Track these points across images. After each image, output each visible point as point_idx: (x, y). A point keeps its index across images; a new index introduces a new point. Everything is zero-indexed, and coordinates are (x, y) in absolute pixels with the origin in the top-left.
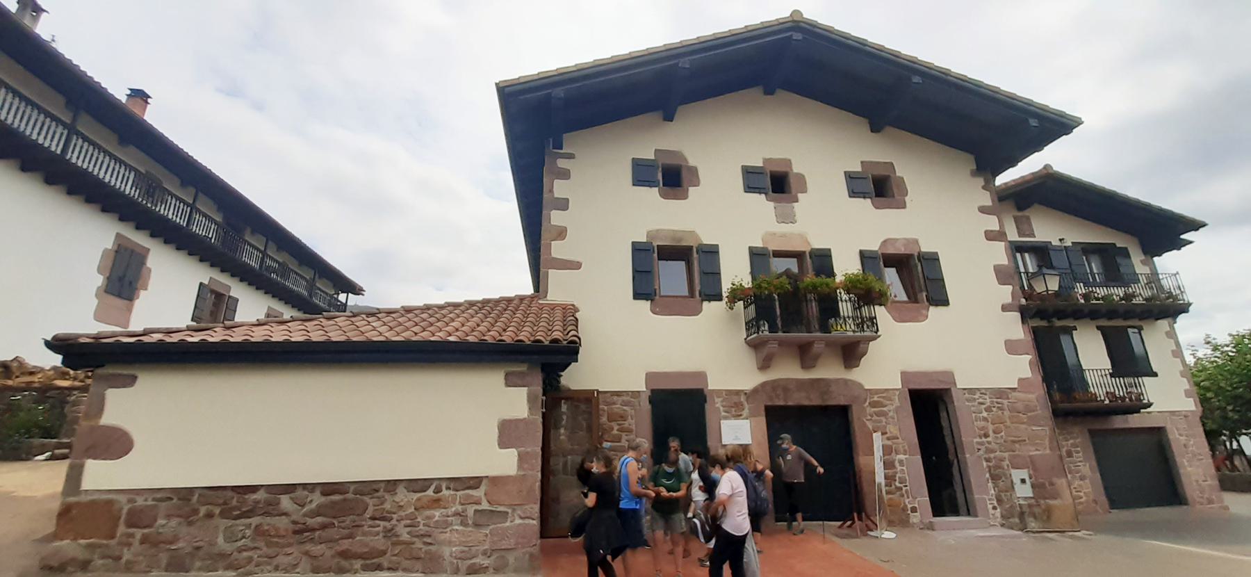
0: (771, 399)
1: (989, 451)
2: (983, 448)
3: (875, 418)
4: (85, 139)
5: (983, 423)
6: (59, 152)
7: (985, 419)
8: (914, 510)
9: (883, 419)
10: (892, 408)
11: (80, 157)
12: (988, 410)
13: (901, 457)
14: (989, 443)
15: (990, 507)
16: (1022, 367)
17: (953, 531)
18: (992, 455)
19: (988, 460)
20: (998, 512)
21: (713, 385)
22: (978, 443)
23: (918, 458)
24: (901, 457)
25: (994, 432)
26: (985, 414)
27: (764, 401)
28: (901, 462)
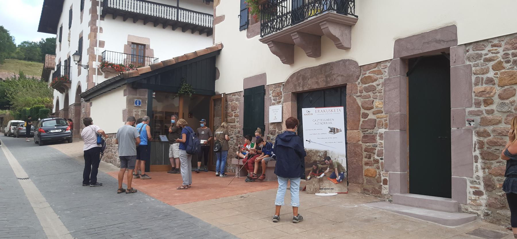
0: (295, 88)
1: (485, 122)
2: (478, 119)
3: (364, 93)
4: (184, 9)
5: (488, 87)
6: (176, 19)
7: (490, 81)
8: (385, 182)
9: (371, 94)
10: (381, 81)
11: (185, 17)
12: (498, 67)
13: (382, 131)
14: (491, 112)
15: (470, 190)
16: (116, 177)
17: (428, 208)
18: (489, 129)
19: (479, 134)
20: (483, 199)
21: (269, 81)
22: (471, 113)
23: (454, 109)
24: (382, 131)
25: (501, 97)
26: (491, 74)
27: (291, 89)
28: (381, 135)
